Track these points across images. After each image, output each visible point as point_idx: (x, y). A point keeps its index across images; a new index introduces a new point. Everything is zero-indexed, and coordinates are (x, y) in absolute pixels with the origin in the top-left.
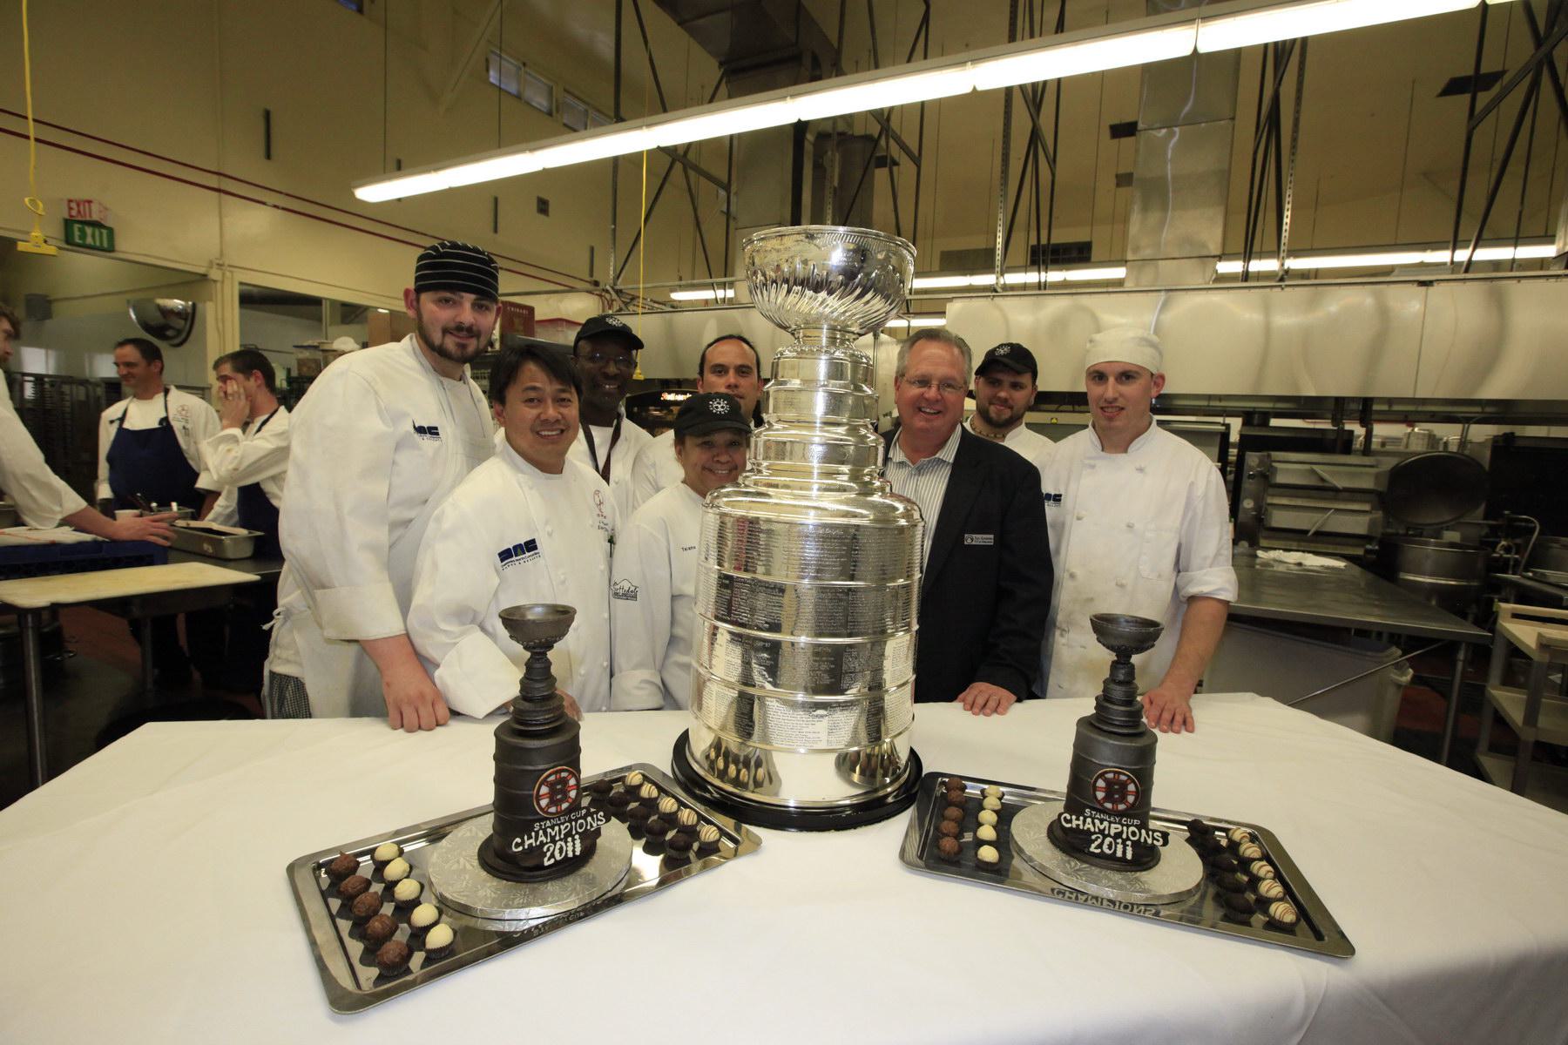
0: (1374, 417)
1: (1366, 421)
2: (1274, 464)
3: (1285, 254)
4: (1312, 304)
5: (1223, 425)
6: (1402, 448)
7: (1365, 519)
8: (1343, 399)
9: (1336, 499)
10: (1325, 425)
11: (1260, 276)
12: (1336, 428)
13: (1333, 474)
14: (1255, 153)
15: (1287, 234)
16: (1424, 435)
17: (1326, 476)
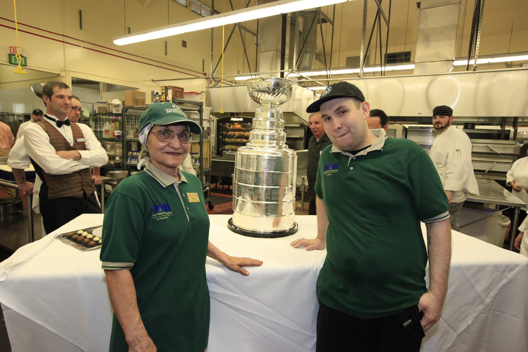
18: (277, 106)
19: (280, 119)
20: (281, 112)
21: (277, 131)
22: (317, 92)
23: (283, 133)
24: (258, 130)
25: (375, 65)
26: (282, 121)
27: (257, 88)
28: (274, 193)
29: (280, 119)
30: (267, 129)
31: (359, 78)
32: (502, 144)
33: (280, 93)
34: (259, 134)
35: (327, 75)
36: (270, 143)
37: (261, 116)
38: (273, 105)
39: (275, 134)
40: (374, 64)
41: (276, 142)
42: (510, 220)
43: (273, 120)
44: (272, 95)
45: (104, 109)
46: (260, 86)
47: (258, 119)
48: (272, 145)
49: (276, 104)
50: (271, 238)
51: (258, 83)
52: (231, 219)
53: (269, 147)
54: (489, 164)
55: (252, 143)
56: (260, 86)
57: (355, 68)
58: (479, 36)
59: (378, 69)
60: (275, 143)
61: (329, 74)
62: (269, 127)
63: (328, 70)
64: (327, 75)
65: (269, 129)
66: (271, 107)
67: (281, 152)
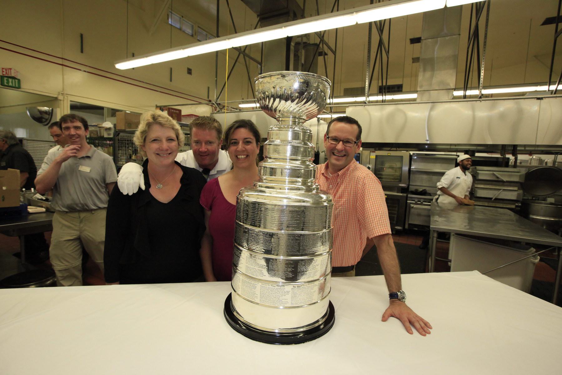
0: (518, 152)
1: (514, 153)
2: (478, 172)
3: (482, 88)
4: (492, 108)
5: (457, 155)
6: (528, 165)
7: (515, 193)
8: (505, 145)
9: (505, 186)
10: (498, 156)
11: (471, 97)
12: (502, 157)
13: (501, 175)
14: (468, 48)
15: (482, 80)
16: (537, 159)
17: (499, 176)
18: (303, 121)
19: (308, 143)
20: (308, 131)
21: (303, 162)
22: (320, 118)
23: (312, 166)
24: (274, 160)
25: (377, 95)
26: (311, 146)
27: (273, 90)
28: (301, 268)
29: (308, 143)
30: (287, 159)
31: (365, 104)
32: (500, 171)
33: (309, 101)
34: (274, 167)
35: (330, 103)
36: (292, 182)
37: (277, 139)
38: (298, 120)
39: (301, 167)
40: (377, 93)
41: (302, 180)
42: (538, 256)
43: (296, 143)
44: (297, 103)
45: (95, 133)
46: (278, 88)
47: (273, 141)
48: (295, 184)
49: (301, 119)
50: (296, 344)
51: (273, 82)
52: (229, 301)
53: (291, 189)
54: (490, 191)
55: (262, 182)
56: (278, 88)
57: (356, 97)
58: (483, 64)
59: (380, 98)
60: (301, 181)
61: (331, 102)
62: (291, 155)
63: (331, 98)
64: (330, 103)
65: (291, 158)
66: (294, 122)
67: (312, 197)
